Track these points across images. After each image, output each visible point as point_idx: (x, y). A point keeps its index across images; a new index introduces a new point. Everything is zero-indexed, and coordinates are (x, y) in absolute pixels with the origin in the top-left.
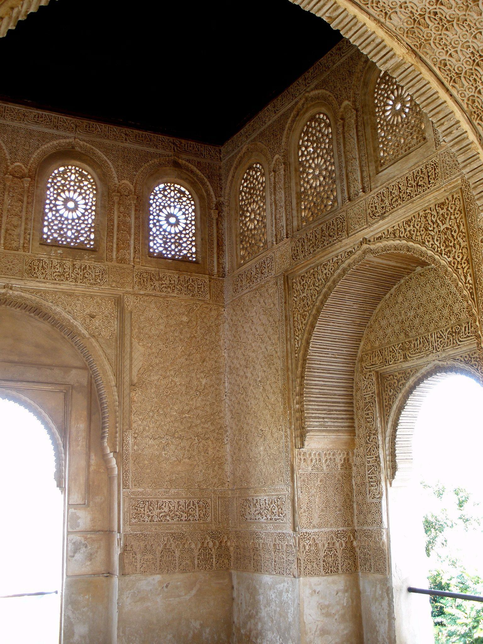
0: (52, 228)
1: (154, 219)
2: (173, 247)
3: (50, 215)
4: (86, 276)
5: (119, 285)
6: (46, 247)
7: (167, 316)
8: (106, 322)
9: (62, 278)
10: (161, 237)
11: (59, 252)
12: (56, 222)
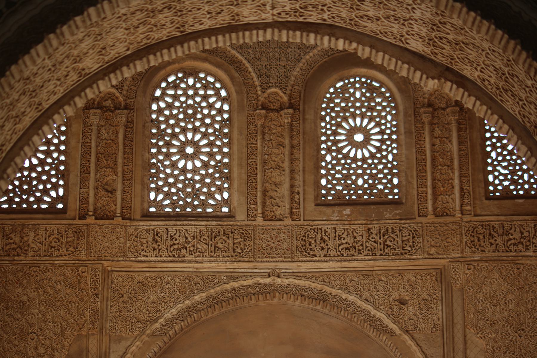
0: (334, 178)
1: (492, 137)
2: (526, 177)
3: (328, 158)
4: (389, 243)
5: (441, 251)
6: (324, 209)
7: (520, 288)
8: (425, 309)
9: (352, 251)
10: (505, 164)
11: (344, 213)
12: (339, 168)
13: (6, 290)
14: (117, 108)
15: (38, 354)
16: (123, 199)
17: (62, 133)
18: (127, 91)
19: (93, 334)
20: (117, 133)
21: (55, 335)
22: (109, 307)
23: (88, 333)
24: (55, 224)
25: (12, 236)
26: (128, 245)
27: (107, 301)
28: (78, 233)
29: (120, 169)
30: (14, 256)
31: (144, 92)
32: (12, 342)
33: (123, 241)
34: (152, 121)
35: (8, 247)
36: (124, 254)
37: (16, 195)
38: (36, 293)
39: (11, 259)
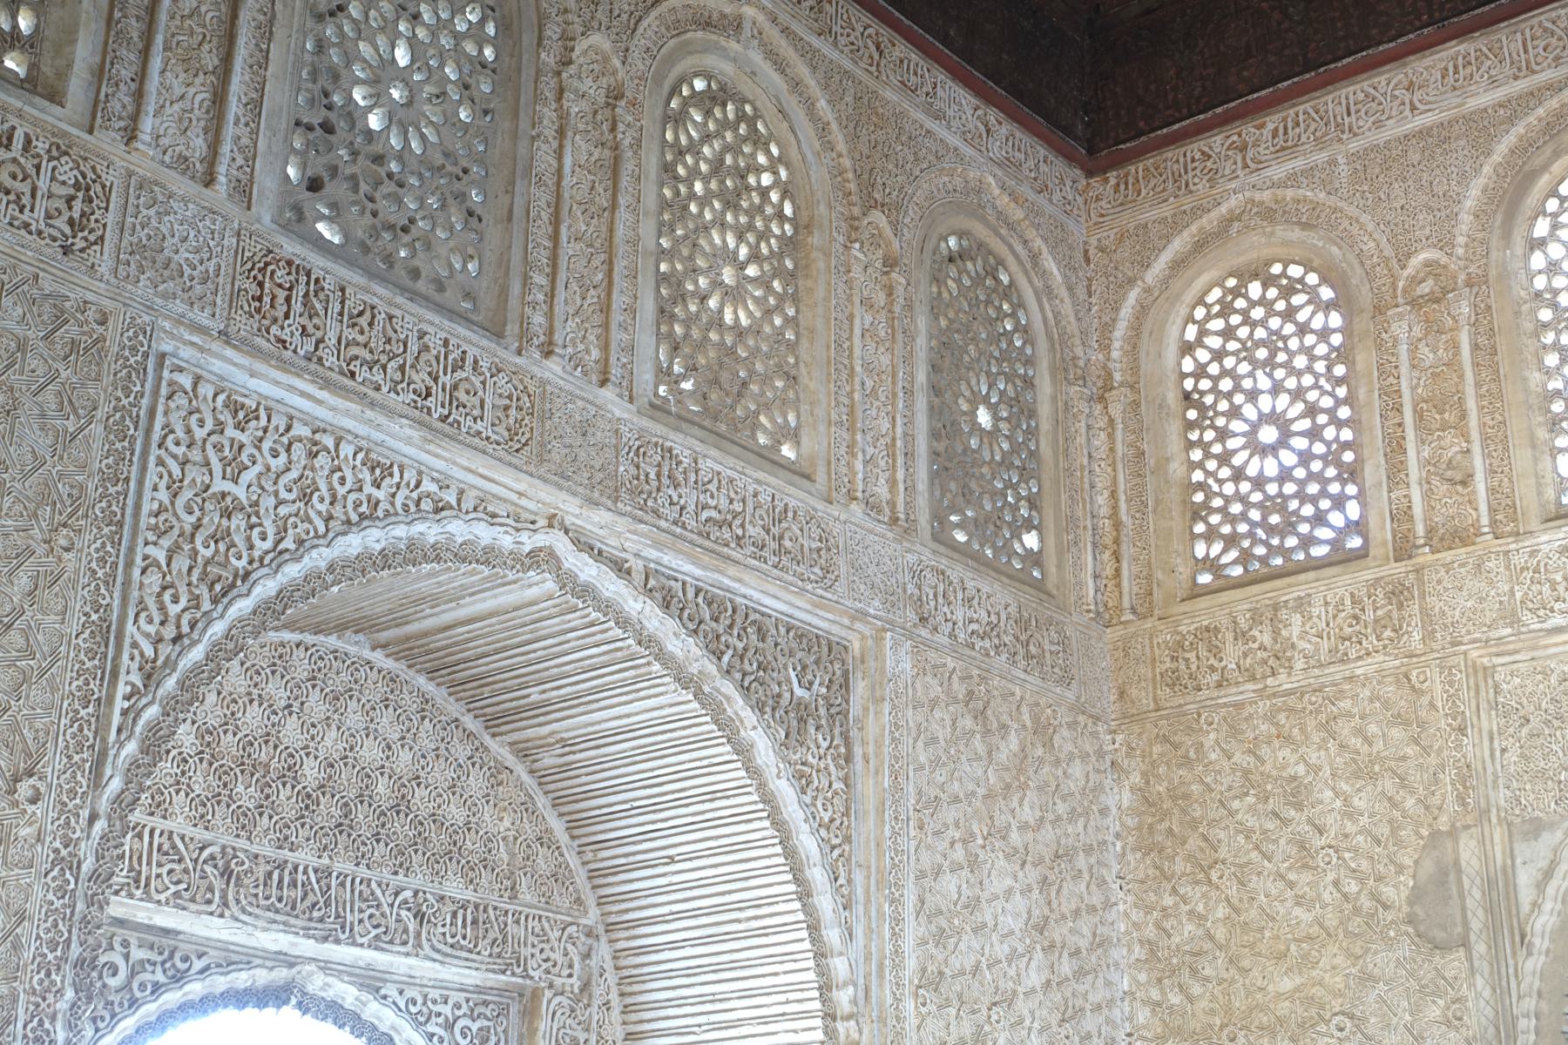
13: (1258, 758)
14: (1445, 291)
15: (1346, 896)
16: (1492, 491)
17: (1339, 381)
18: (1467, 245)
19: (1467, 827)
20: (1455, 346)
21: (1378, 842)
22: (1498, 753)
23: (1453, 825)
24: (1343, 584)
25: (1255, 633)
26: (1518, 595)
27: (1491, 739)
28: (1398, 594)
29: (1473, 421)
30: (1264, 677)
31: (1507, 236)
32: (1282, 877)
33: (1507, 588)
34: (1538, 295)
35: (1248, 660)
36: (1514, 620)
37: (1256, 542)
38: (1322, 753)
39: (1260, 686)
